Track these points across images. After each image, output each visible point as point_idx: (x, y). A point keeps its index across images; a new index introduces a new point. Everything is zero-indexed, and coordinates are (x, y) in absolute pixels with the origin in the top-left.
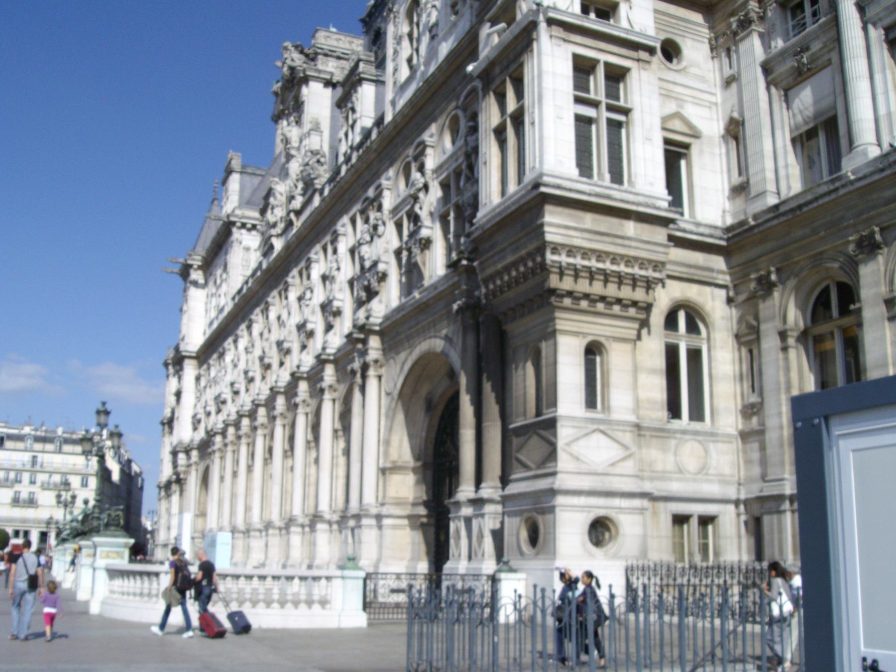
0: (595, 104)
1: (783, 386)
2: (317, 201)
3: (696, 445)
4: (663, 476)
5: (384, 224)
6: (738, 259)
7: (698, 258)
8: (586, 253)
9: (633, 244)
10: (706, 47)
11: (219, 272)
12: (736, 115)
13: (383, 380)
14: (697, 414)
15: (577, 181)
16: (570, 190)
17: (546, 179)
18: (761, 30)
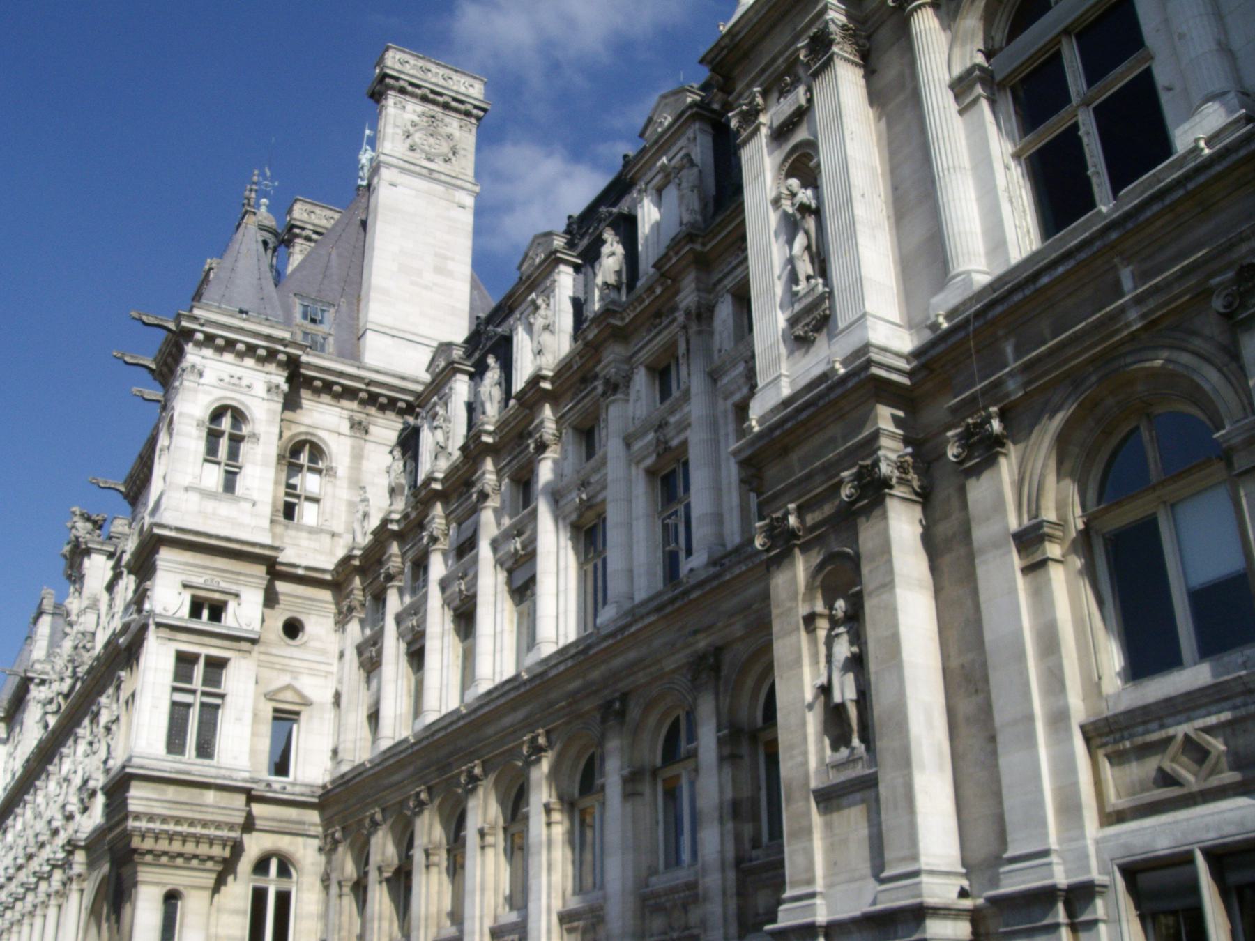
0: (193, 692)
5: (99, 741)
6: (329, 812)
7: (292, 813)
8: (165, 819)
9: (211, 810)
10: (330, 621)
11: (17, 729)
13: (85, 893)
15: (164, 760)
17: (136, 761)
18: (362, 616)
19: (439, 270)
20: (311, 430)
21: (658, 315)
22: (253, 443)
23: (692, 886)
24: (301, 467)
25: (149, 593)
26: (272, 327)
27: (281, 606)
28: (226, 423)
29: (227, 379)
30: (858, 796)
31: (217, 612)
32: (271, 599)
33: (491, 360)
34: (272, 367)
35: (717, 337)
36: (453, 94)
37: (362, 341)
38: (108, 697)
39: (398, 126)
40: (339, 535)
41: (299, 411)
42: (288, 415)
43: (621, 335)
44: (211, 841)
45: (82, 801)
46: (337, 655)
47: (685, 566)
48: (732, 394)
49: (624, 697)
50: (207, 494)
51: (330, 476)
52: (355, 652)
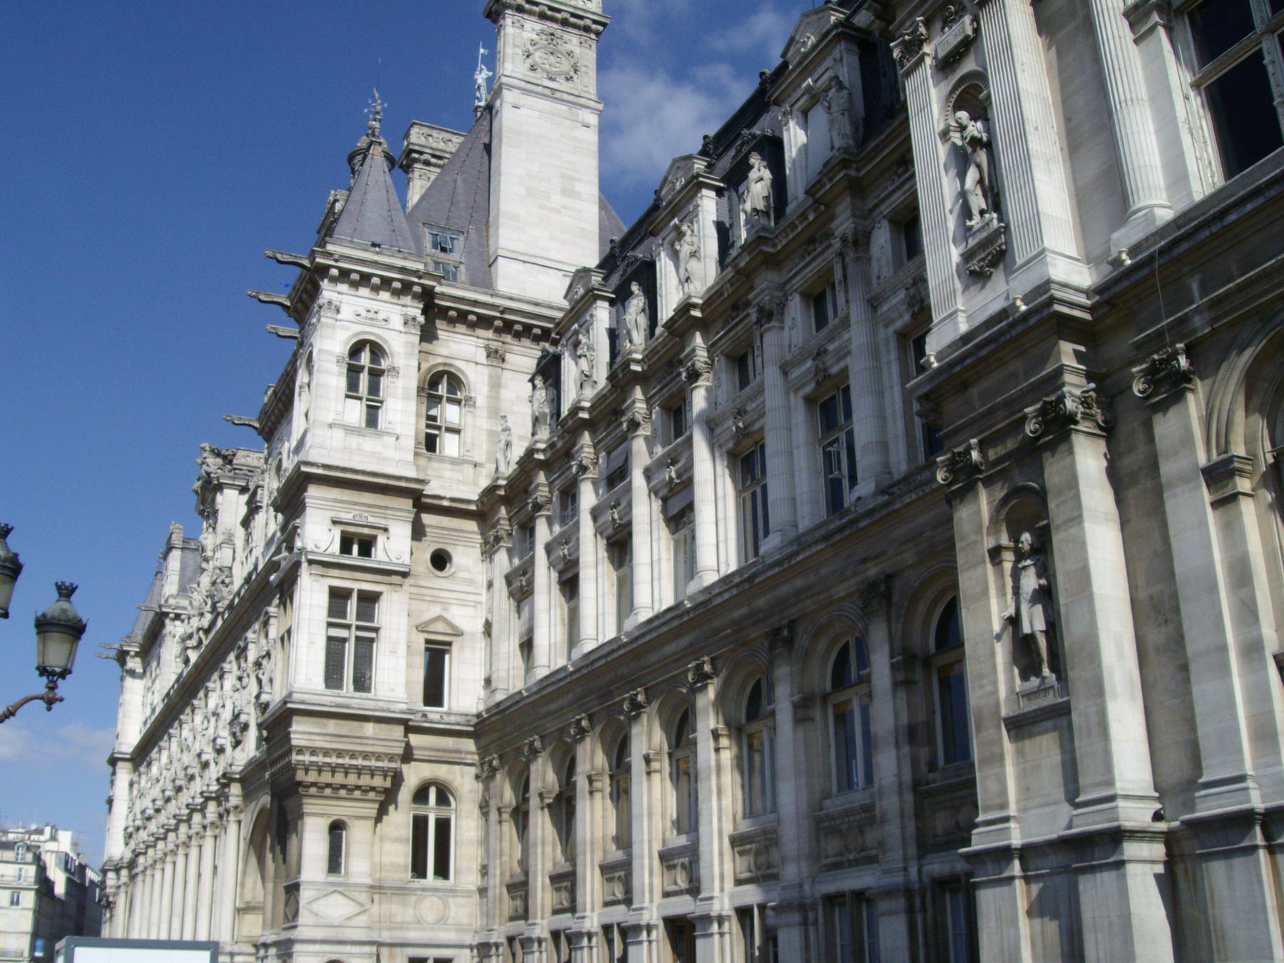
0: (348, 627)
1: (498, 853)
2: (220, 622)
3: (435, 900)
4: (402, 926)
5: (248, 676)
6: (483, 742)
7: (449, 742)
8: (327, 753)
9: (371, 742)
10: (477, 552)
11: (154, 664)
13: (243, 824)
14: (442, 870)
16: (313, 704)
17: (296, 697)
18: (509, 545)
19: (567, 192)
20: (448, 361)
21: (812, 241)
22: (393, 376)
23: (868, 809)
24: (440, 398)
25: (299, 531)
26: (405, 258)
27: (428, 538)
28: (365, 358)
29: (364, 313)
30: (1050, 724)
31: (367, 547)
32: (418, 532)
33: (635, 288)
34: (407, 300)
35: (874, 264)
36: (571, 10)
37: (493, 268)
38: (254, 632)
39: (517, 46)
40: (482, 465)
41: (435, 342)
42: (426, 346)
43: (773, 262)
44: (372, 772)
45: (234, 734)
46: (485, 585)
47: (849, 499)
48: (892, 321)
49: (792, 625)
50: (350, 430)
51: (470, 406)
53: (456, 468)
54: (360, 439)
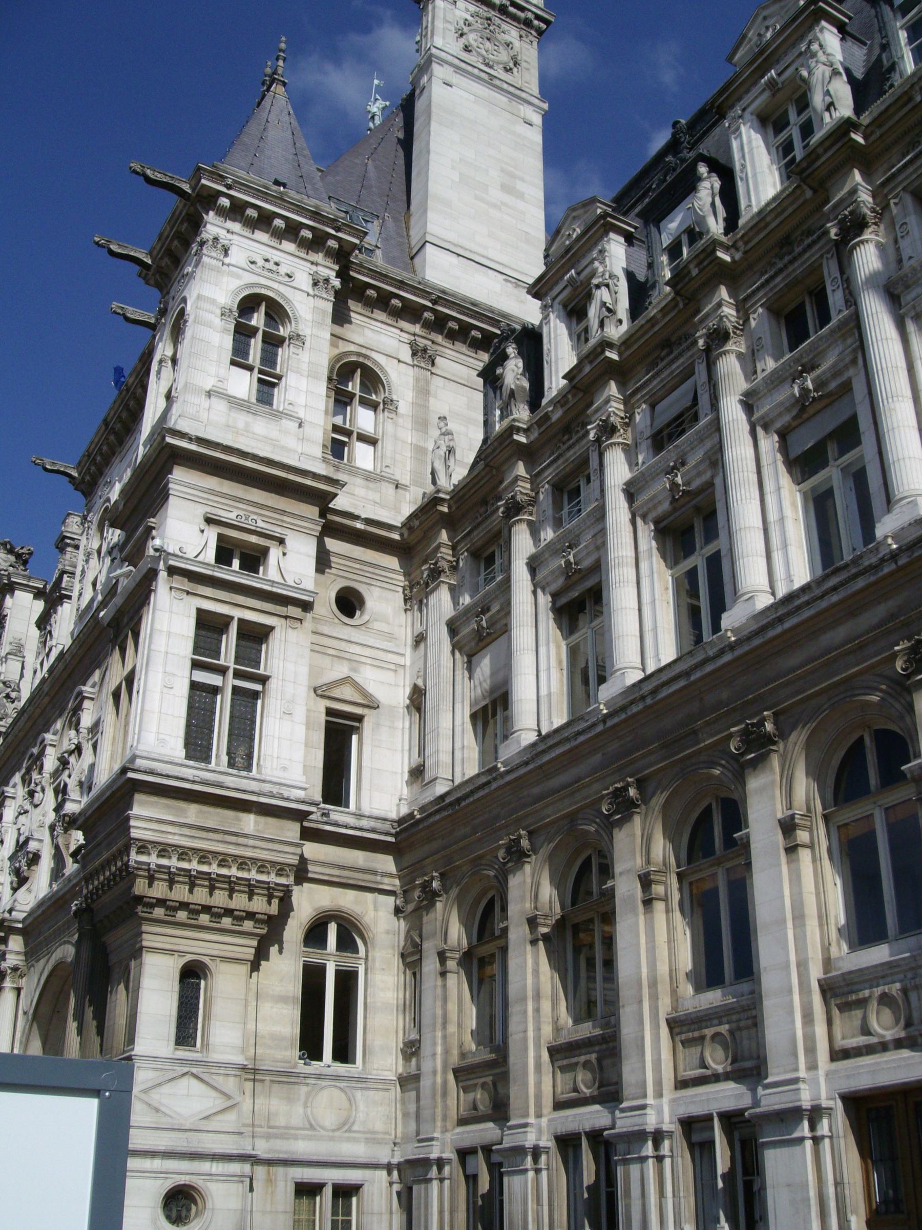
0: (222, 671)
1: (439, 1021)
4: (286, 1133)
5: (43, 790)
6: (409, 859)
7: (358, 857)
8: (184, 853)
9: (251, 842)
10: (400, 597)
12: (420, 683)
13: (23, 993)
14: (343, 1053)
15: (182, 765)
16: (168, 776)
17: (139, 763)
19: (507, 189)
20: (363, 351)
24: (352, 396)
25: (154, 533)
27: (333, 571)
28: (258, 320)
29: (261, 262)
32: (323, 562)
34: (319, 257)
37: (416, 260)
38: (55, 734)
40: (405, 487)
41: (347, 326)
42: (338, 330)
44: (251, 889)
45: (17, 872)
46: (409, 641)
50: (235, 403)
51: (390, 411)
52: (445, 630)
53: (372, 485)
54: (250, 418)
